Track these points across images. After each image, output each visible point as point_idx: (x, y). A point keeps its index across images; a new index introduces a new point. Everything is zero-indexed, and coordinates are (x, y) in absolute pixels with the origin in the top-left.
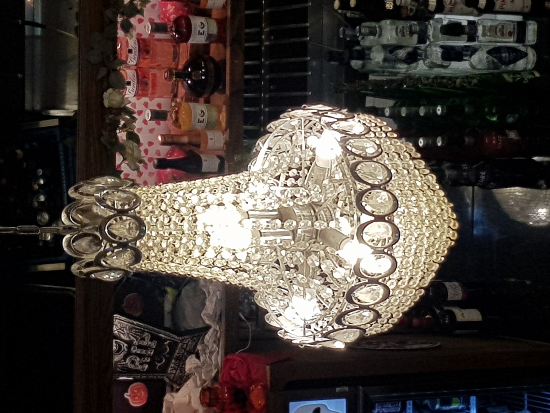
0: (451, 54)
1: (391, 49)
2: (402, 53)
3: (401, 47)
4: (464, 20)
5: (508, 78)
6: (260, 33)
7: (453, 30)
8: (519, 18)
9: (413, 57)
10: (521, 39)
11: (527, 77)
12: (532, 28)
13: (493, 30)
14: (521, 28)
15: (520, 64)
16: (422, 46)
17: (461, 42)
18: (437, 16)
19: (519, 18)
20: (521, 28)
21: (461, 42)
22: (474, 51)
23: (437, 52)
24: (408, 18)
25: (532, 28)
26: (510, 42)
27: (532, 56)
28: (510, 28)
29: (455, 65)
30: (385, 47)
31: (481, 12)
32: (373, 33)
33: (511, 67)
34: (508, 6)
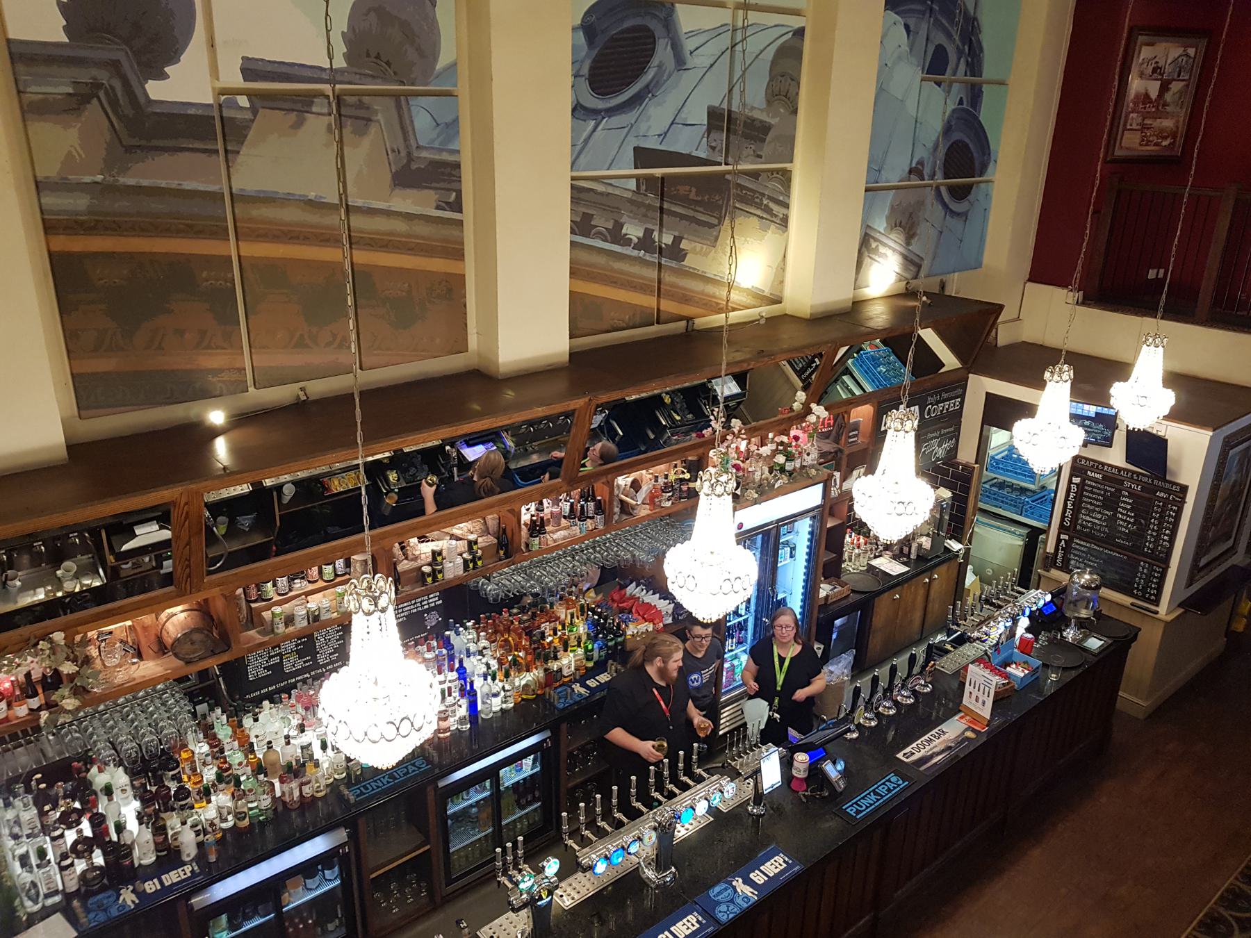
0: (24, 860)
1: (17, 822)
2: (16, 830)
3: (20, 826)
4: (50, 856)
5: (17, 902)
6: (6, 743)
7: (42, 853)
8: (61, 888)
9: (15, 837)
10: (47, 896)
11: (21, 913)
12: (57, 899)
13: (49, 879)
14: (56, 892)
15: (28, 903)
16: (24, 839)
17: (34, 860)
18: (48, 838)
19: (61, 888)
20: (56, 892)
21: (34, 860)
22: (31, 872)
23: (20, 851)
24: (42, 823)
25: (57, 899)
26: (43, 890)
27: (37, 908)
28: (51, 886)
29: (17, 864)
30: (18, 816)
31: (59, 864)
32: (25, 806)
33: (25, 899)
34: (66, 879)
